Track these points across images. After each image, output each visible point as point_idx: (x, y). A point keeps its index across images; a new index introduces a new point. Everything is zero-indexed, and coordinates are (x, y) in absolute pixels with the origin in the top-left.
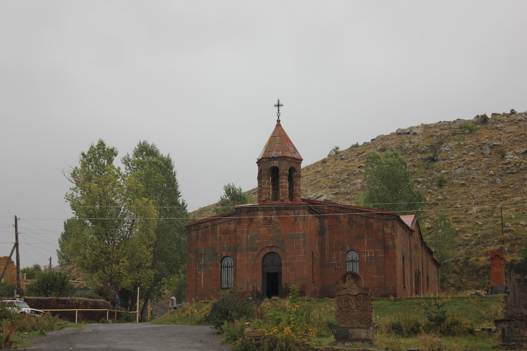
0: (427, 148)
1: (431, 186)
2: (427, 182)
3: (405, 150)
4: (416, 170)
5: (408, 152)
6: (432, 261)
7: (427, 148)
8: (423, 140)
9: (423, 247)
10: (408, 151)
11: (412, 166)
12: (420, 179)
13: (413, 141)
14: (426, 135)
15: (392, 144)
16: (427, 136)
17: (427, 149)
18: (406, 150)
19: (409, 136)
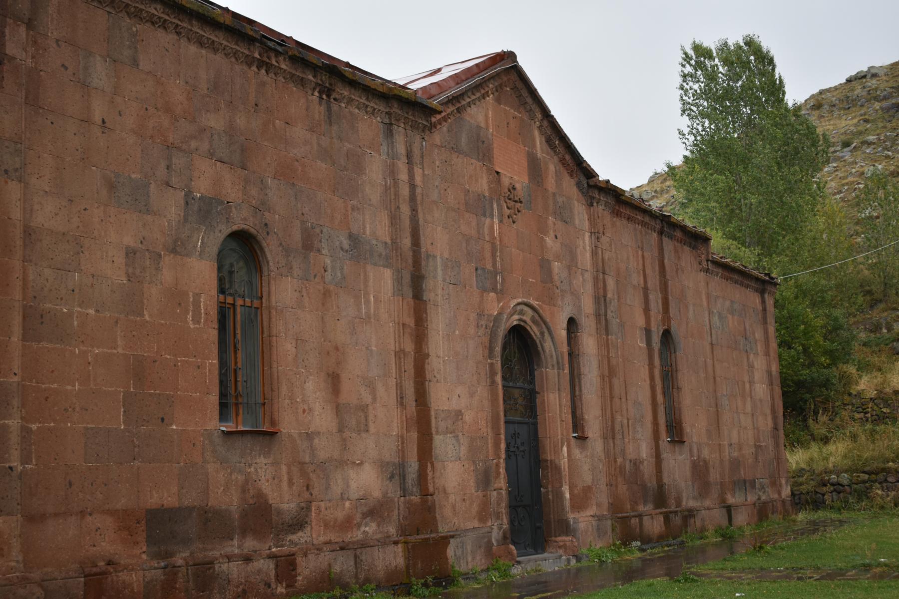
0: (891, 90)
1: (891, 147)
2: (884, 142)
3: (853, 101)
4: (868, 126)
5: (859, 103)
6: (707, 271)
7: (891, 90)
8: (887, 81)
9: (600, 209)
10: (859, 101)
11: (861, 122)
12: (871, 138)
13: (870, 84)
14: (892, 74)
15: (833, 96)
16: (895, 75)
17: (891, 93)
18: (856, 99)
19: (864, 80)
